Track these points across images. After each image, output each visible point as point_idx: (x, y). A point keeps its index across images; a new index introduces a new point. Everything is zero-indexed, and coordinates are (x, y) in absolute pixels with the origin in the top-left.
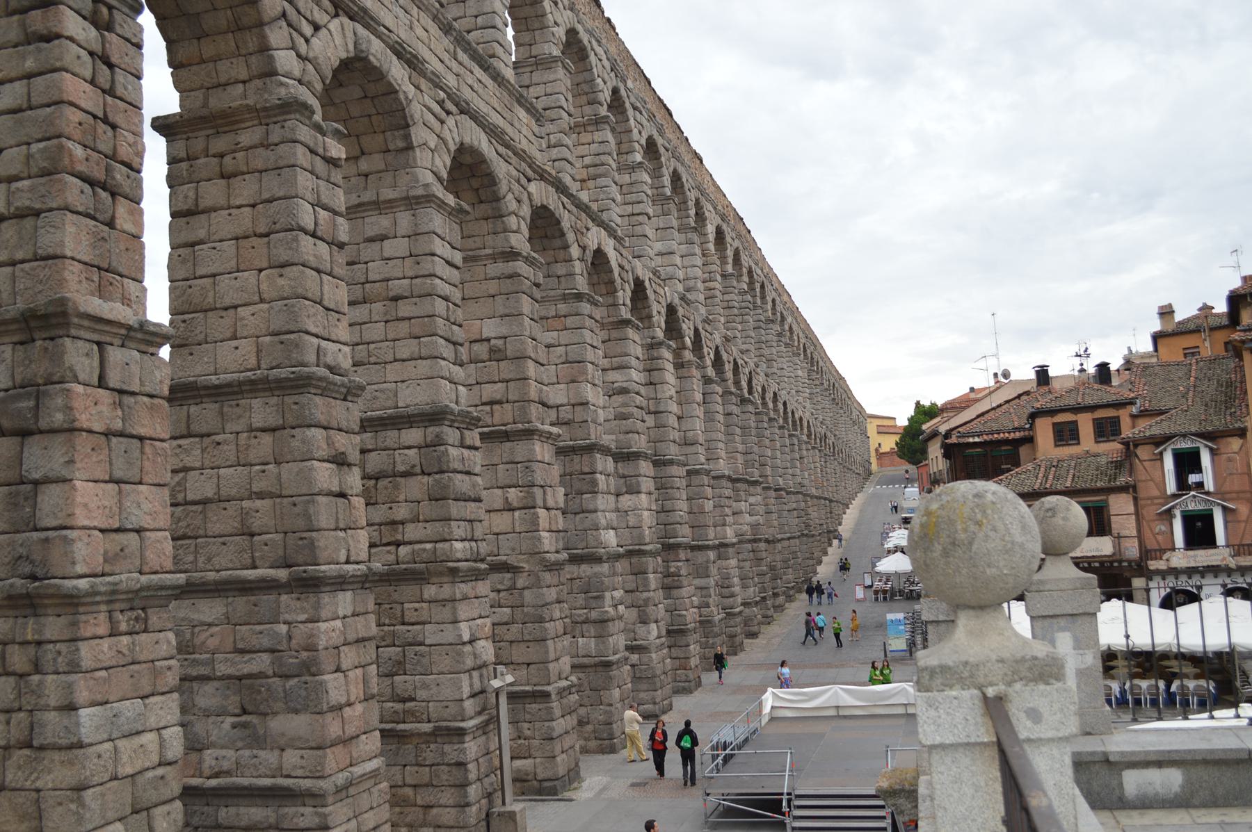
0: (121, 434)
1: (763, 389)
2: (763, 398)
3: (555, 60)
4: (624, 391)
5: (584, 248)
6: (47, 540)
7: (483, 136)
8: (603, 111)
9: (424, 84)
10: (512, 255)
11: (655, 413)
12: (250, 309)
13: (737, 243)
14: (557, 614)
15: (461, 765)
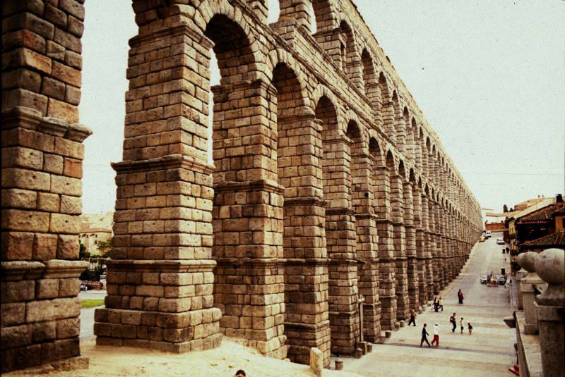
0: (274, 218)
1: (443, 199)
2: (442, 202)
3: (377, 84)
4: (396, 201)
5: (385, 151)
6: (256, 247)
7: (356, 116)
8: (391, 100)
9: (341, 101)
10: (364, 156)
11: (405, 209)
12: (295, 178)
13: (434, 143)
14: (375, 279)
15: (348, 326)
